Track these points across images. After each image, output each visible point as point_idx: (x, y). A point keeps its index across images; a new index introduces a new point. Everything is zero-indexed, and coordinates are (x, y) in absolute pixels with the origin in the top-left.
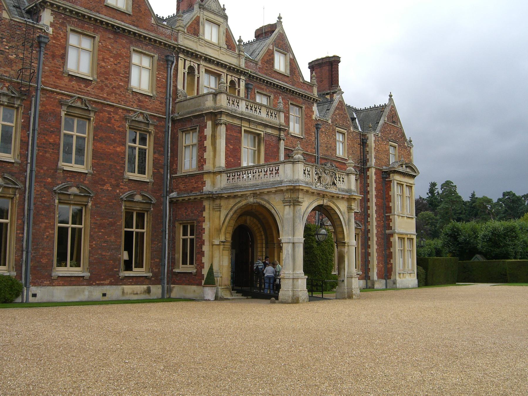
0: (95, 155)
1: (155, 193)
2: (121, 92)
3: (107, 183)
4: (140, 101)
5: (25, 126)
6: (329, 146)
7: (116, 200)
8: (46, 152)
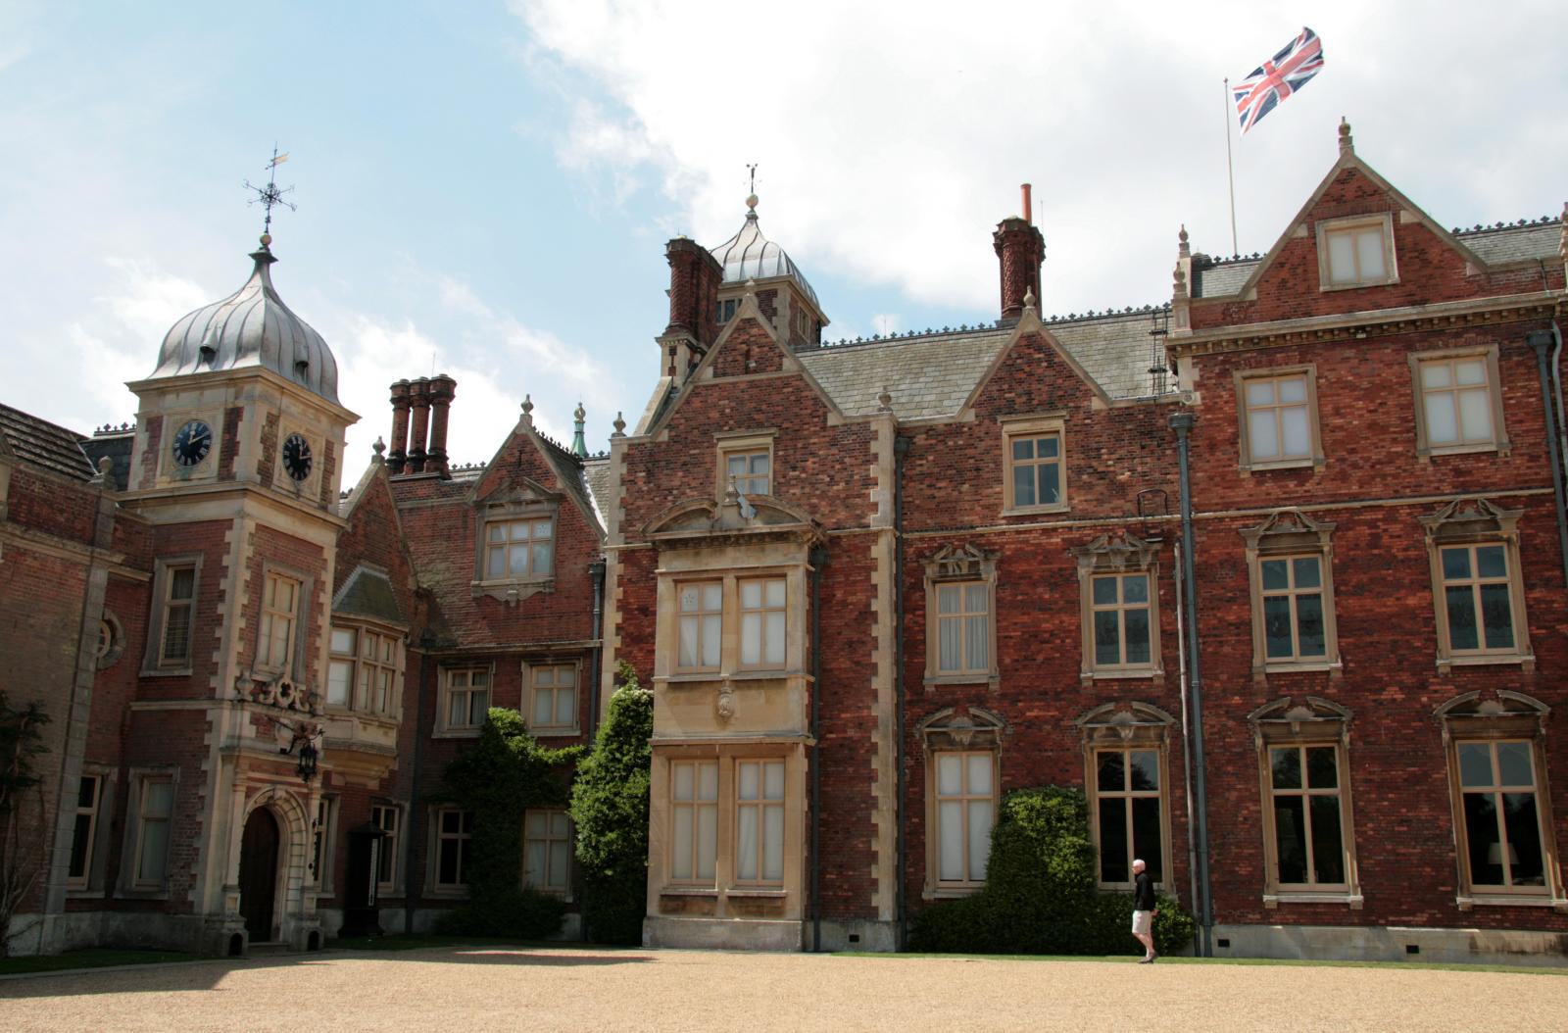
0: (1344, 626)
1: (1548, 688)
2: (1399, 468)
3: (1388, 685)
4: (1458, 472)
5: (1166, 604)
7: (1421, 720)
8: (1221, 644)
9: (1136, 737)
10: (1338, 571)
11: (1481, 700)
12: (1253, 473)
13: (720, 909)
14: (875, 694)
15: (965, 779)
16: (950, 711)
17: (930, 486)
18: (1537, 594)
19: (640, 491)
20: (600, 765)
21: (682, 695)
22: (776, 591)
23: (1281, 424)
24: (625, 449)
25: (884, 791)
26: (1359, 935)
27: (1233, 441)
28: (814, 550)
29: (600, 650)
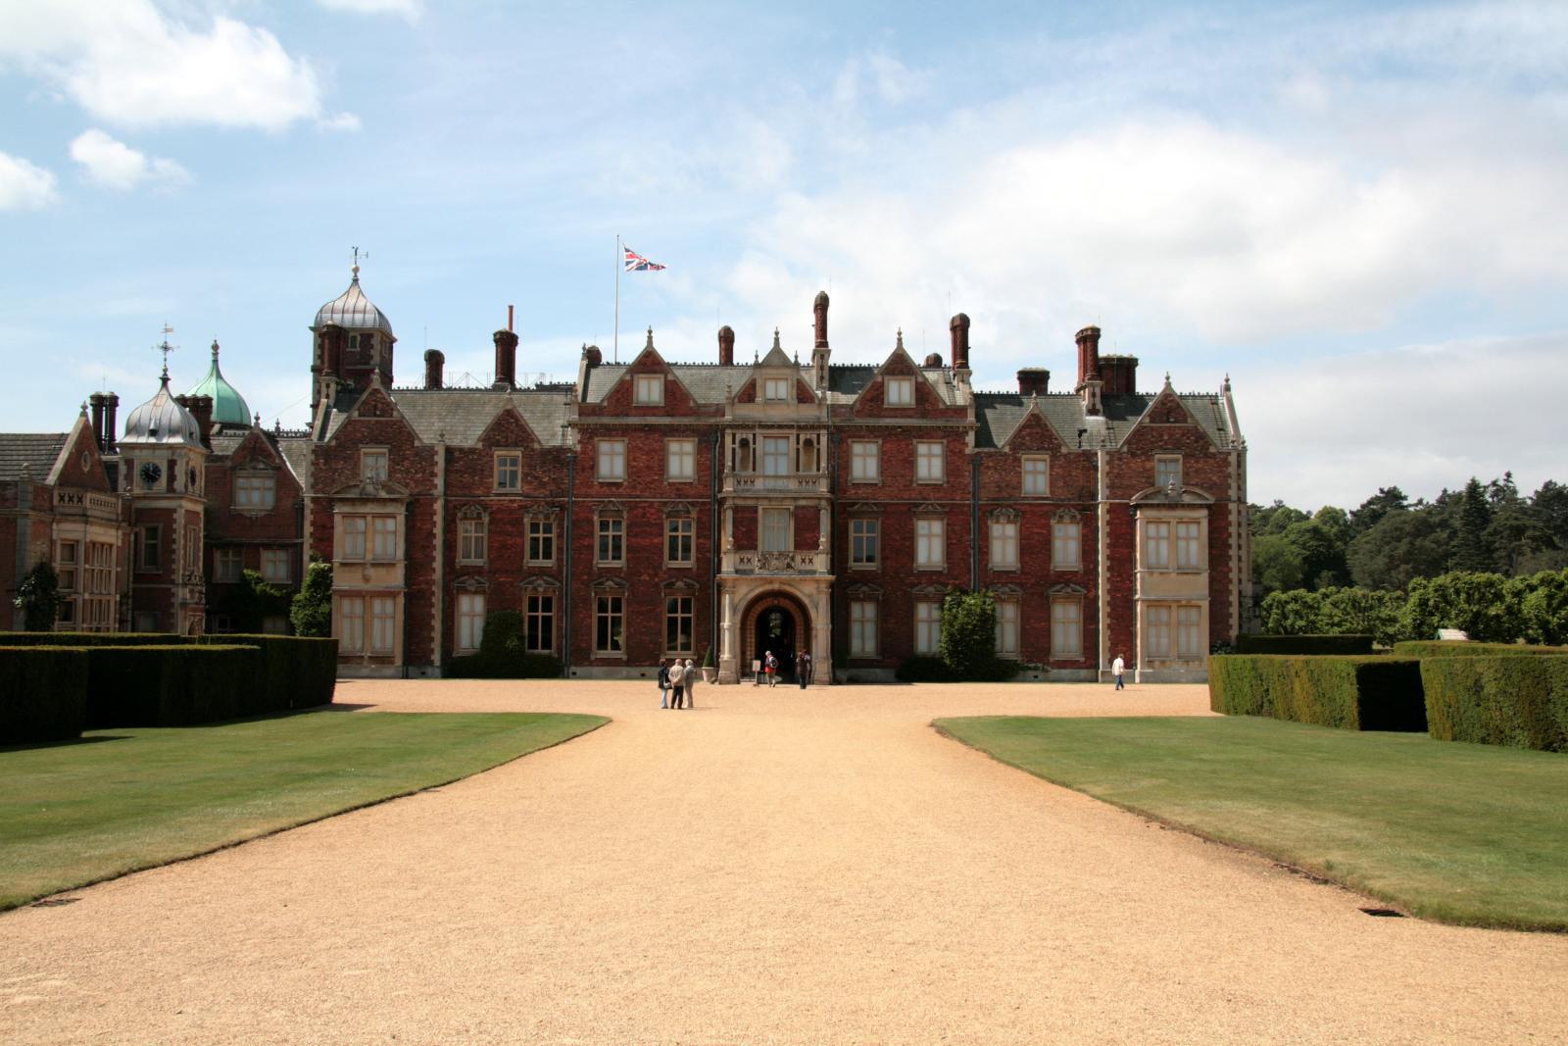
4: (678, 489)
5: (560, 536)
6: (1004, 485)
9: (545, 591)
10: (629, 527)
11: (677, 581)
12: (600, 483)
13: (365, 663)
14: (434, 570)
15: (472, 605)
16: (466, 577)
17: (461, 476)
18: (701, 541)
19: (321, 469)
20: (306, 598)
21: (347, 569)
22: (390, 524)
23: (612, 462)
24: (313, 448)
25: (437, 611)
26: (625, 670)
27: (592, 467)
28: (408, 505)
29: (302, 544)
